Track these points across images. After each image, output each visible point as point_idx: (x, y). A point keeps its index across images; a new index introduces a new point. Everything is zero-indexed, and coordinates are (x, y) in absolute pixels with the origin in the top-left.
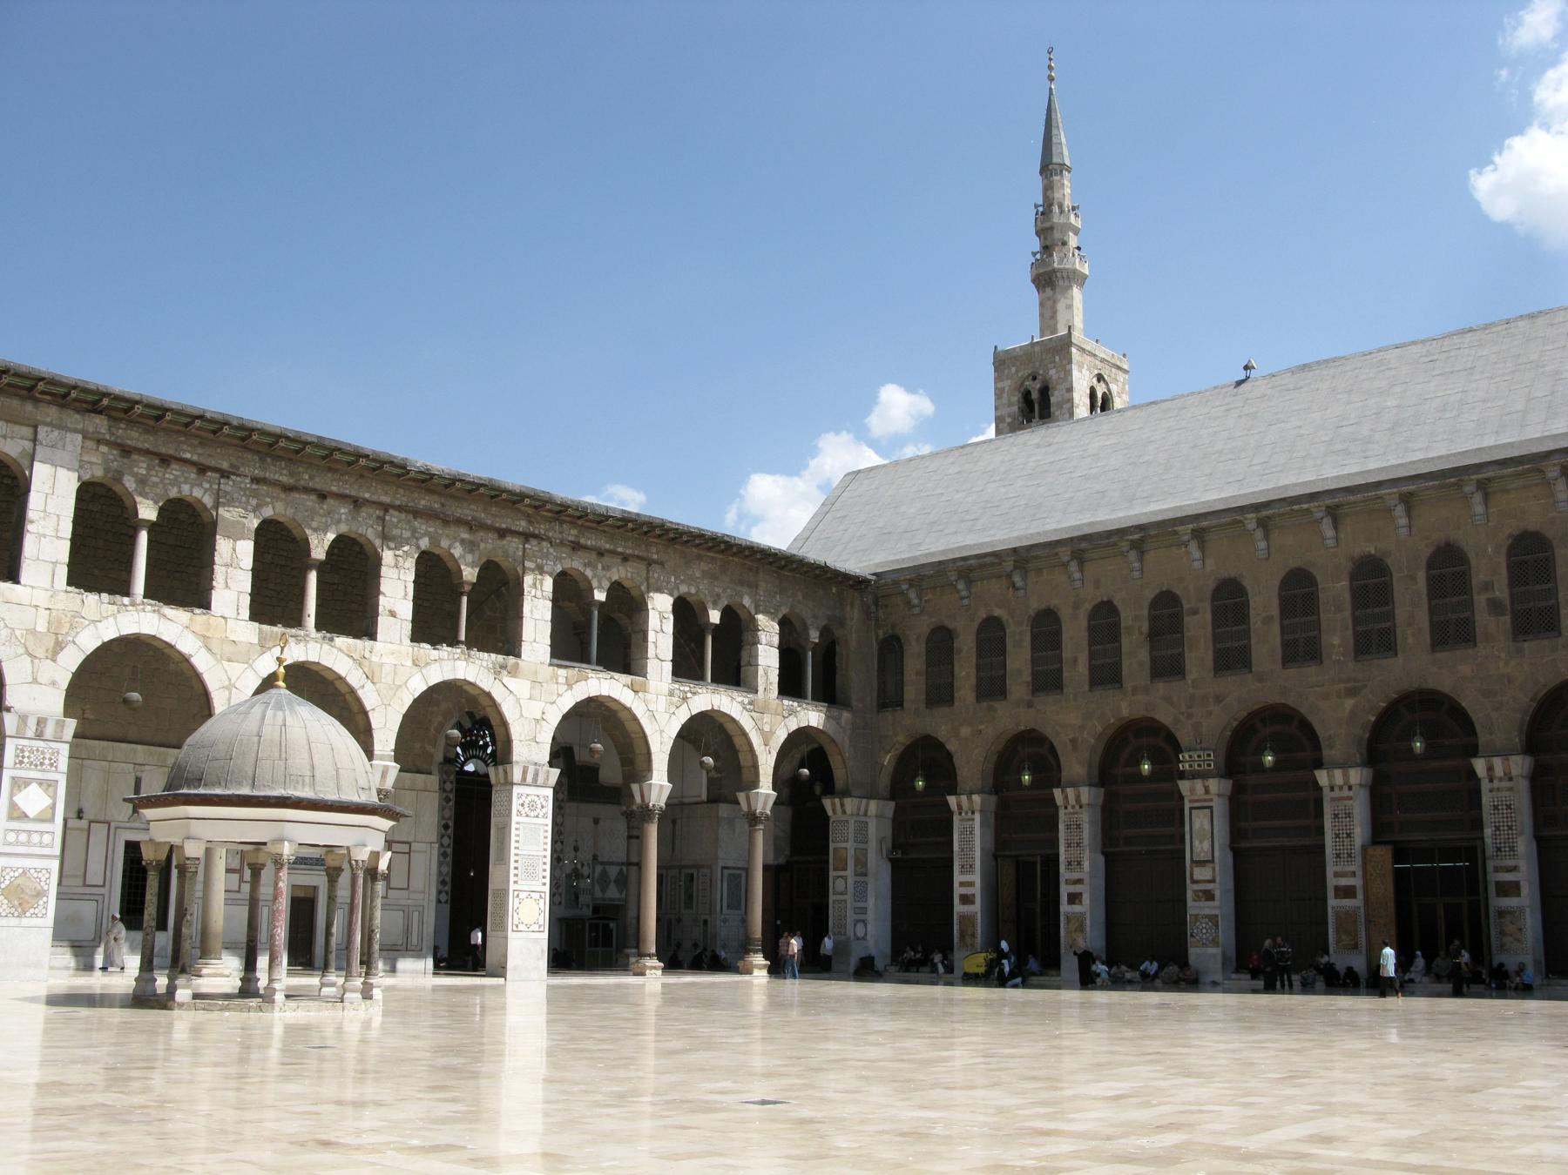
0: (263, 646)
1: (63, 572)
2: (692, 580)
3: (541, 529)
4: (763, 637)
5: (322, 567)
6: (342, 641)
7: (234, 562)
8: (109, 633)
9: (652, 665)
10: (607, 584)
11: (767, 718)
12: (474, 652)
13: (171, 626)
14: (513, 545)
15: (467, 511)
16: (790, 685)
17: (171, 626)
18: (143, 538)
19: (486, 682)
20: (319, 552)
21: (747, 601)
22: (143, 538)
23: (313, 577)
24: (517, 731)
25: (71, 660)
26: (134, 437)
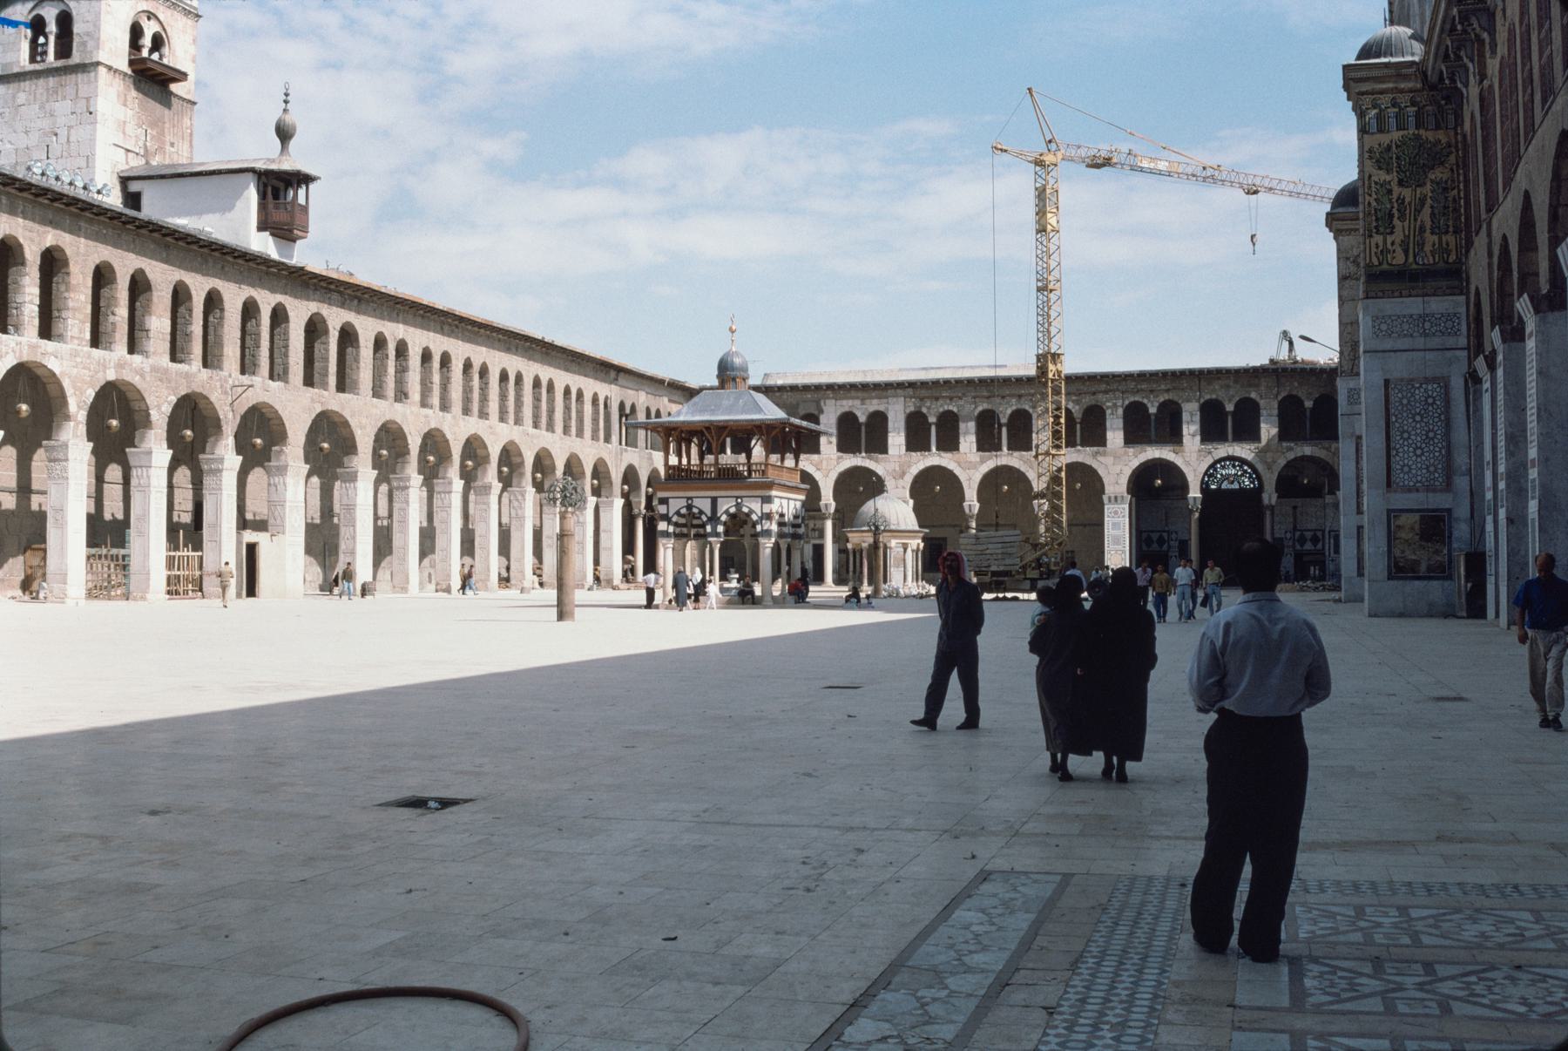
0: (982, 461)
2: (1214, 391)
4: (1263, 412)
6: (1016, 454)
8: (921, 466)
9: (1186, 439)
13: (945, 460)
14: (1100, 396)
16: (1287, 432)
17: (945, 460)
18: (933, 429)
19: (1088, 461)
20: (1004, 420)
21: (1253, 395)
22: (933, 429)
24: (1105, 481)
25: (909, 479)
26: (924, 393)
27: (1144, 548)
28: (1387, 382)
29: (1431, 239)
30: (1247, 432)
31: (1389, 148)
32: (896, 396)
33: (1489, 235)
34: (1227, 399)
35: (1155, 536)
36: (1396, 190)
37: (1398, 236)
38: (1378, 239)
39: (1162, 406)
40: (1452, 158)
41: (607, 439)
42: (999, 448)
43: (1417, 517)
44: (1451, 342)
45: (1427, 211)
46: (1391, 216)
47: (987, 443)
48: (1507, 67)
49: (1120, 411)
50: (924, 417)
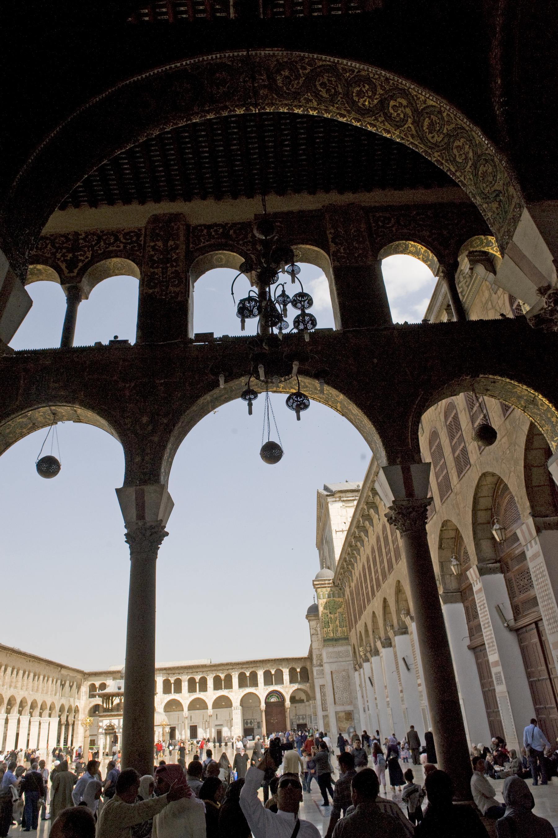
0: (190, 696)
1: (162, 693)
2: (267, 667)
3: (235, 667)
5: (199, 683)
6: (202, 693)
7: (185, 686)
8: (168, 699)
10: (249, 673)
11: (287, 689)
12: (226, 690)
14: (230, 671)
15: (220, 668)
16: (292, 681)
18: (173, 685)
20: (197, 681)
22: (173, 685)
23: (198, 684)
25: (164, 704)
26: (170, 672)
27: (246, 726)
28: (332, 672)
29: (340, 629)
30: (280, 681)
31: (326, 603)
32: (160, 673)
33: (356, 630)
34: (272, 669)
35: (249, 721)
36: (329, 615)
37: (331, 628)
38: (325, 629)
39: (251, 673)
40: (343, 606)
41: (55, 695)
42: (196, 691)
43: (343, 714)
44: (347, 659)
45: (338, 621)
46: (328, 622)
47: (192, 689)
48: (357, 587)
49: (237, 676)
50: (169, 681)
